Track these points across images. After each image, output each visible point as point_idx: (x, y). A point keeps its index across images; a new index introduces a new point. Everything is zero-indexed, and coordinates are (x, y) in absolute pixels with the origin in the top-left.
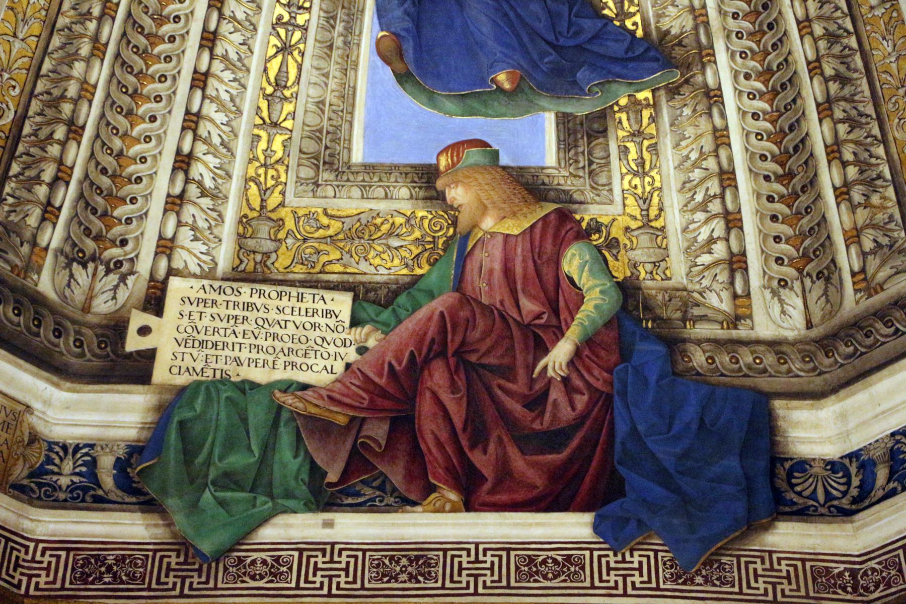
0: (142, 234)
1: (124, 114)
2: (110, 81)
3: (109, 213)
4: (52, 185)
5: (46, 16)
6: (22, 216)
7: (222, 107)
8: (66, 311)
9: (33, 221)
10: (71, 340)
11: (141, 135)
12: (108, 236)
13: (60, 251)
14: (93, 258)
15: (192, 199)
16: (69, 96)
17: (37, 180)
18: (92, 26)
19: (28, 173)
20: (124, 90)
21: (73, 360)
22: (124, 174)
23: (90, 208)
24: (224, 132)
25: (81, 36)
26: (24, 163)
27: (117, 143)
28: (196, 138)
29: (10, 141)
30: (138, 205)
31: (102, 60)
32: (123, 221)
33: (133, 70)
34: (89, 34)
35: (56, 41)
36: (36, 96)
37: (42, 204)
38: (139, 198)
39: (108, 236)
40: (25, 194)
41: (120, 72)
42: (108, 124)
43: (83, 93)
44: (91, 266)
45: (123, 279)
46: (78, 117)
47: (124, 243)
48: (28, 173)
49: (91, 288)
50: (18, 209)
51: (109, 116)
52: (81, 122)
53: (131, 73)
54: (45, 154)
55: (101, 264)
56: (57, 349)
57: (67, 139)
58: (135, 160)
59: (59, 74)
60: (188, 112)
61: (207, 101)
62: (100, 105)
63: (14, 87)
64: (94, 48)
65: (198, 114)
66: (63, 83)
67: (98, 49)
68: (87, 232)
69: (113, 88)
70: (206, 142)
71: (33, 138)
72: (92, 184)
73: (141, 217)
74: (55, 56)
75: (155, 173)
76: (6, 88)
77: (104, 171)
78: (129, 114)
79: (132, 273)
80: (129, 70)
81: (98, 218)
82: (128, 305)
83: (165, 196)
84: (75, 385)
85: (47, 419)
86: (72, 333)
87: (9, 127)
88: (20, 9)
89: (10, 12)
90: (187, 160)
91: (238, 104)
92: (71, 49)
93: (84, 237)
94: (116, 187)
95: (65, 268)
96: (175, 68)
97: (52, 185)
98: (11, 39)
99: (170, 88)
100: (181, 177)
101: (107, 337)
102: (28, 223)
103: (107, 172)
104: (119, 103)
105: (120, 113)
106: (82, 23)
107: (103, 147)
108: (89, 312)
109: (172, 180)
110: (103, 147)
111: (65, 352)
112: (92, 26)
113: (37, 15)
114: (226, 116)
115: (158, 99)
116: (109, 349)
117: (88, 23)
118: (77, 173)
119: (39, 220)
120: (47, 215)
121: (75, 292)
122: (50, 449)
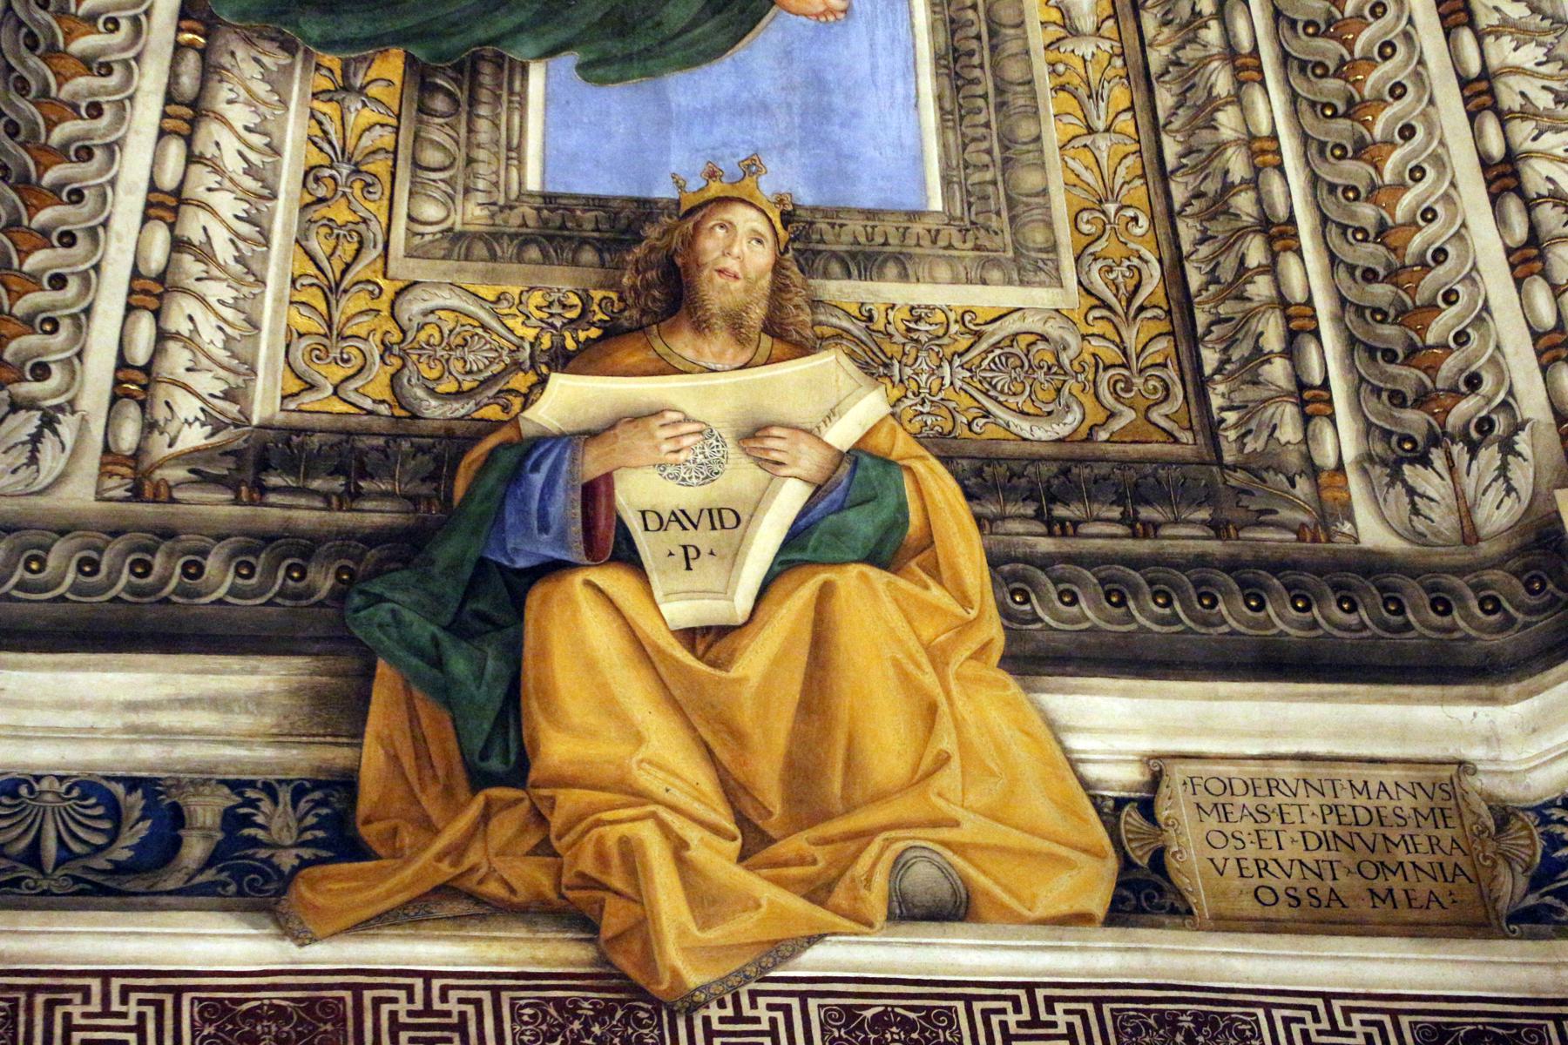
0: (1498, 347)
1: (1350, 154)
2: (1295, 112)
3: (1420, 344)
4: (1291, 351)
5: (1125, 64)
6: (1265, 434)
7: (1522, 34)
8: (1436, 559)
9: (1289, 432)
10: (1474, 605)
11: (1401, 174)
12: (1439, 385)
13: (1367, 460)
14: (1434, 440)
15: (1556, 233)
16: (1237, 181)
17: (1259, 355)
18: (1212, 34)
19: (1240, 352)
20: (1329, 113)
21: (1497, 640)
22: (1408, 261)
23: (1379, 355)
24: (1551, 77)
25: (1204, 62)
26: (1220, 340)
27: (1367, 213)
28: (1503, 118)
29: (1176, 316)
30: (1464, 299)
31: (1263, 83)
32: (1452, 344)
33: (1326, 68)
34: (1215, 51)
35: (1165, 99)
36: (1179, 213)
37: (1290, 394)
38: (1459, 288)
39: (1439, 385)
40: (1252, 393)
41: (1305, 85)
42: (1332, 188)
43: (1260, 159)
44: (1437, 456)
45: (1507, 447)
46: (1272, 206)
47: (1474, 382)
48: (1236, 354)
49: (1459, 495)
50: (1253, 425)
51: (1326, 173)
52: (1282, 212)
53: (1325, 75)
54: (1248, 305)
55: (1453, 442)
56: (1457, 635)
57: (1274, 257)
58: (1415, 223)
59: (1200, 151)
60: (1464, 82)
61: (1490, 40)
62: (1300, 164)
63: (1135, 219)
64: (1237, 70)
65: (1486, 74)
66: (1215, 163)
67: (1246, 68)
68: (1397, 398)
69: (1308, 119)
70: (1524, 115)
71: (1212, 288)
72: (1360, 310)
73: (1479, 319)
74: (1176, 124)
75: (1464, 225)
76: (1122, 226)
77: (1370, 275)
78: (1361, 148)
79: (1518, 427)
80: (1319, 71)
81: (1402, 364)
82: (1543, 489)
83: (1503, 256)
84: (1527, 683)
85: (1507, 768)
86: (1469, 593)
87: (1161, 293)
88: (1076, 81)
89: (1062, 94)
90: (1509, 169)
91: (1549, 11)
92: (1199, 96)
93: (1396, 413)
94: (1405, 291)
95: (1391, 484)
96: (1399, 18)
97: (1291, 351)
98: (1088, 140)
99: (1410, 58)
100: (1513, 205)
101: (1539, 567)
102: (1283, 440)
103: (1375, 273)
104: (1331, 141)
105: (1342, 157)
106: (1194, 40)
107: (1344, 234)
108: (1478, 540)
109: (1501, 220)
110: (1344, 234)
111: (1473, 633)
112: (1212, 34)
113: (1110, 73)
114: (1539, 44)
115: (1398, 91)
116: (1550, 586)
117: (1203, 33)
118: (1324, 306)
119: (1299, 423)
120: (1309, 409)
121: (1433, 516)
122: (1545, 820)
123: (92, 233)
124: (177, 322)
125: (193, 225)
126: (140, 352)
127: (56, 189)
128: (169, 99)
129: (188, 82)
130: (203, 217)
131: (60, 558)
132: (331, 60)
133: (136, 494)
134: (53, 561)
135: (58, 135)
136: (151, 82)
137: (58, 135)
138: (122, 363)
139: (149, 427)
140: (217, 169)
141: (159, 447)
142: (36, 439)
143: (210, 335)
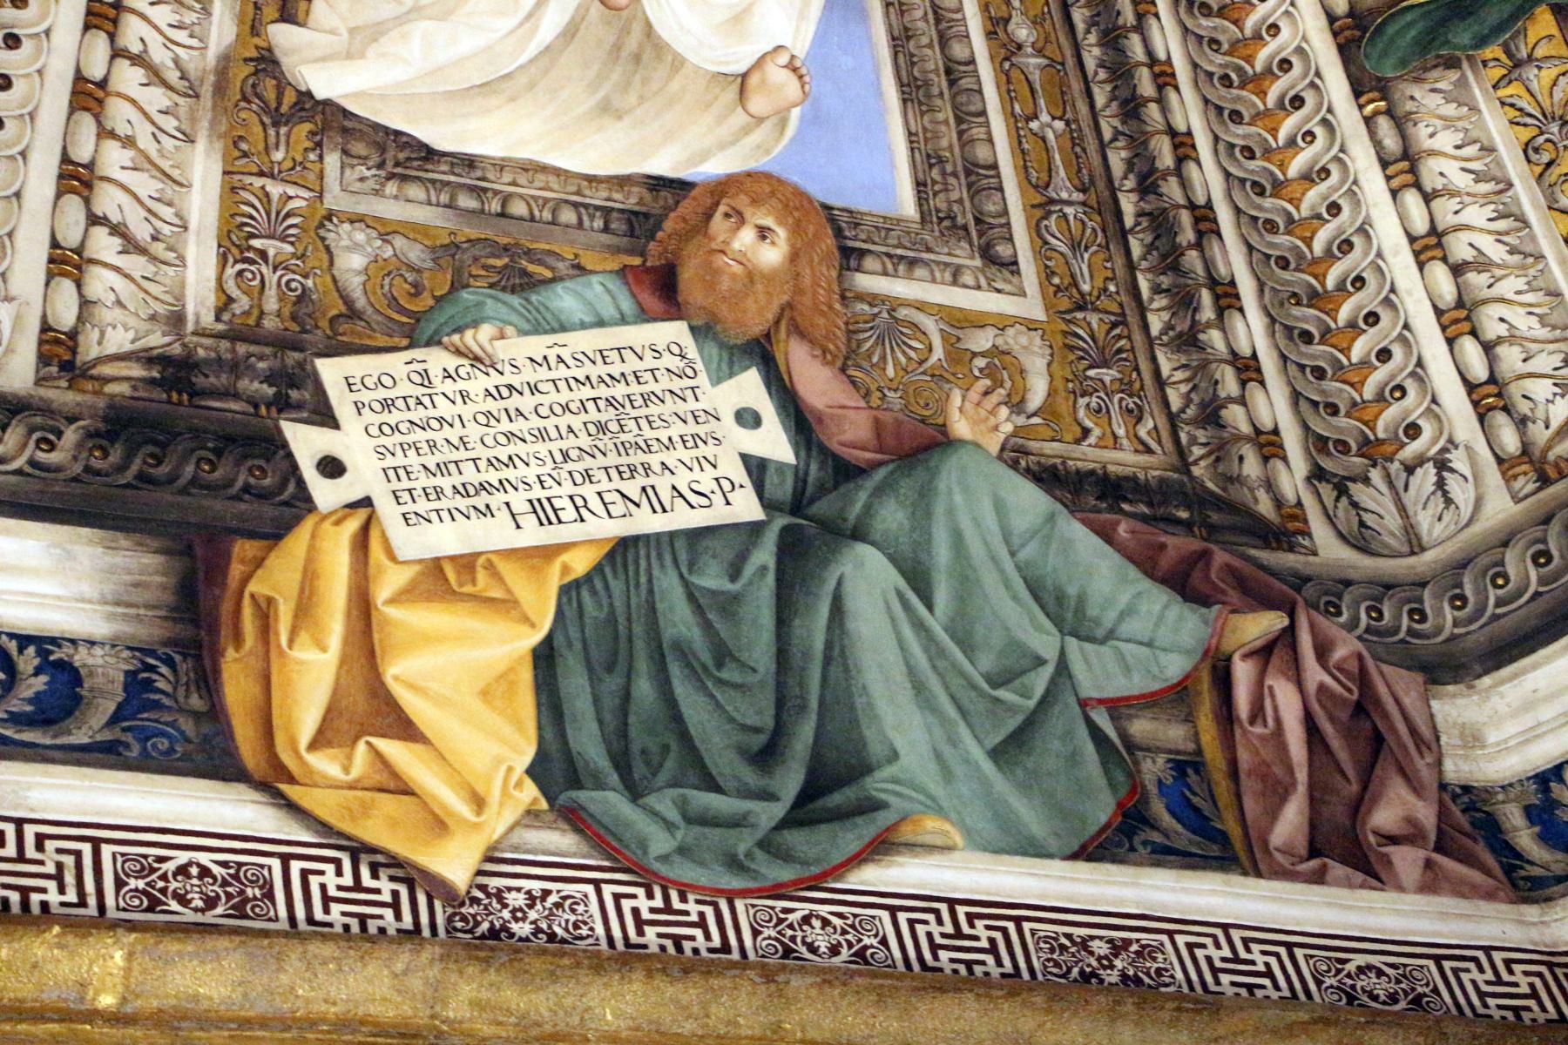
123: (1387, 302)
124: (1493, 330)
125: (1460, 248)
126: (1479, 371)
127: (1341, 287)
128: (1384, 164)
129: (1391, 142)
130: (1465, 237)
131: (1516, 563)
132: (1493, 51)
133: (1544, 481)
134: (1511, 570)
135: (1318, 246)
136: (1363, 160)
137: (1318, 246)
138: (1470, 387)
139: (1522, 423)
140: (1453, 194)
141: (1539, 434)
142: (1440, 484)
143: (1525, 324)
